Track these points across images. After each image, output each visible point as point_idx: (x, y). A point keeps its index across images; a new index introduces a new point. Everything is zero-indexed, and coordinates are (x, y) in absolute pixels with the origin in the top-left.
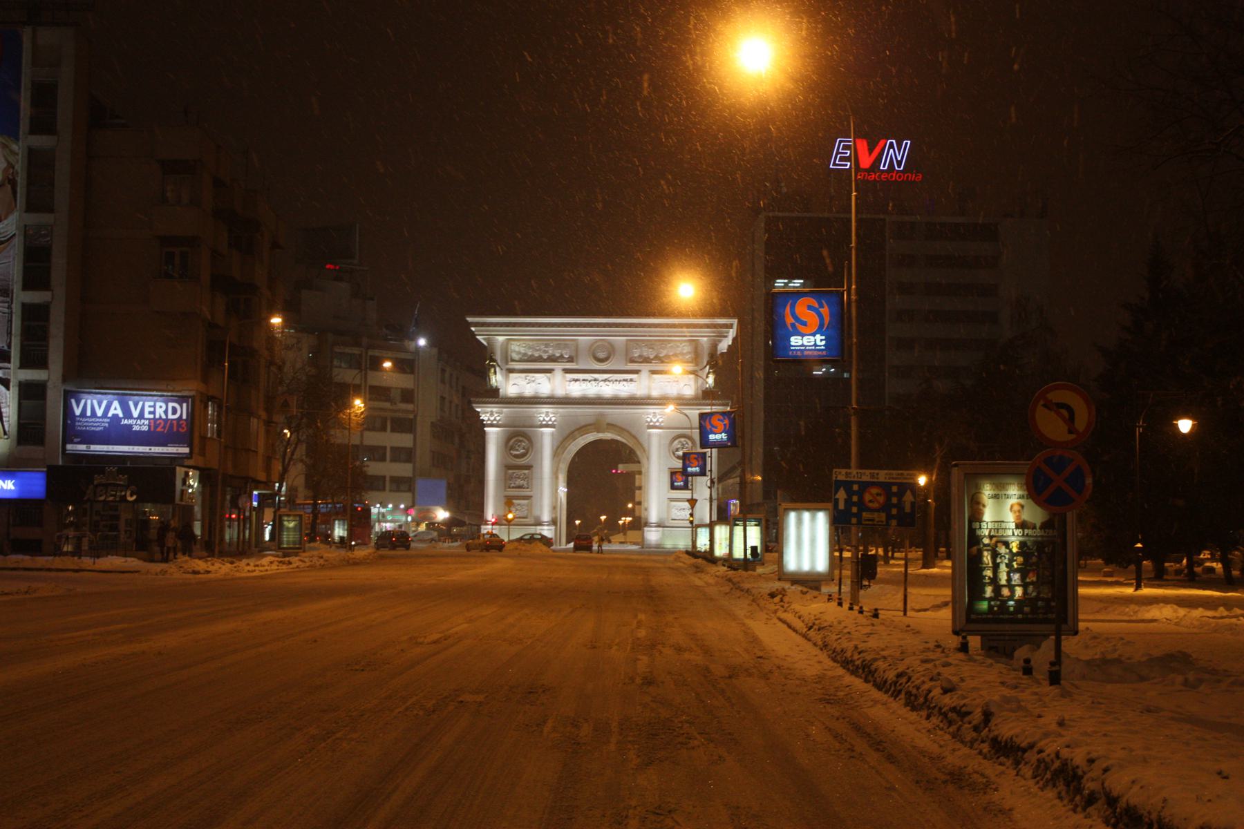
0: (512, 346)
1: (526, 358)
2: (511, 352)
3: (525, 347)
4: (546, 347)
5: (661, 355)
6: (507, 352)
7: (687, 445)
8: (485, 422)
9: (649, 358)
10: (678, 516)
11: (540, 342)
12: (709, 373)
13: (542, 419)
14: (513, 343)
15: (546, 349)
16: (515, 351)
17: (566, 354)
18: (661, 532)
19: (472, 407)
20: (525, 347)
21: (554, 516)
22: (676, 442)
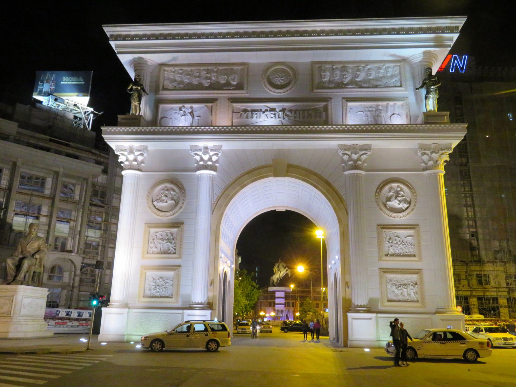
0: (166, 72)
1: (182, 86)
2: (164, 80)
3: (181, 74)
4: (207, 73)
5: (358, 80)
6: (158, 77)
7: (402, 193)
8: (122, 165)
9: (342, 83)
10: (397, 295)
11: (202, 68)
12: (428, 93)
13: (198, 158)
14: (167, 69)
15: (209, 75)
16: (168, 79)
17: (233, 80)
18: (374, 320)
19: (103, 139)
20: (181, 74)
21: (211, 294)
22: (387, 188)
